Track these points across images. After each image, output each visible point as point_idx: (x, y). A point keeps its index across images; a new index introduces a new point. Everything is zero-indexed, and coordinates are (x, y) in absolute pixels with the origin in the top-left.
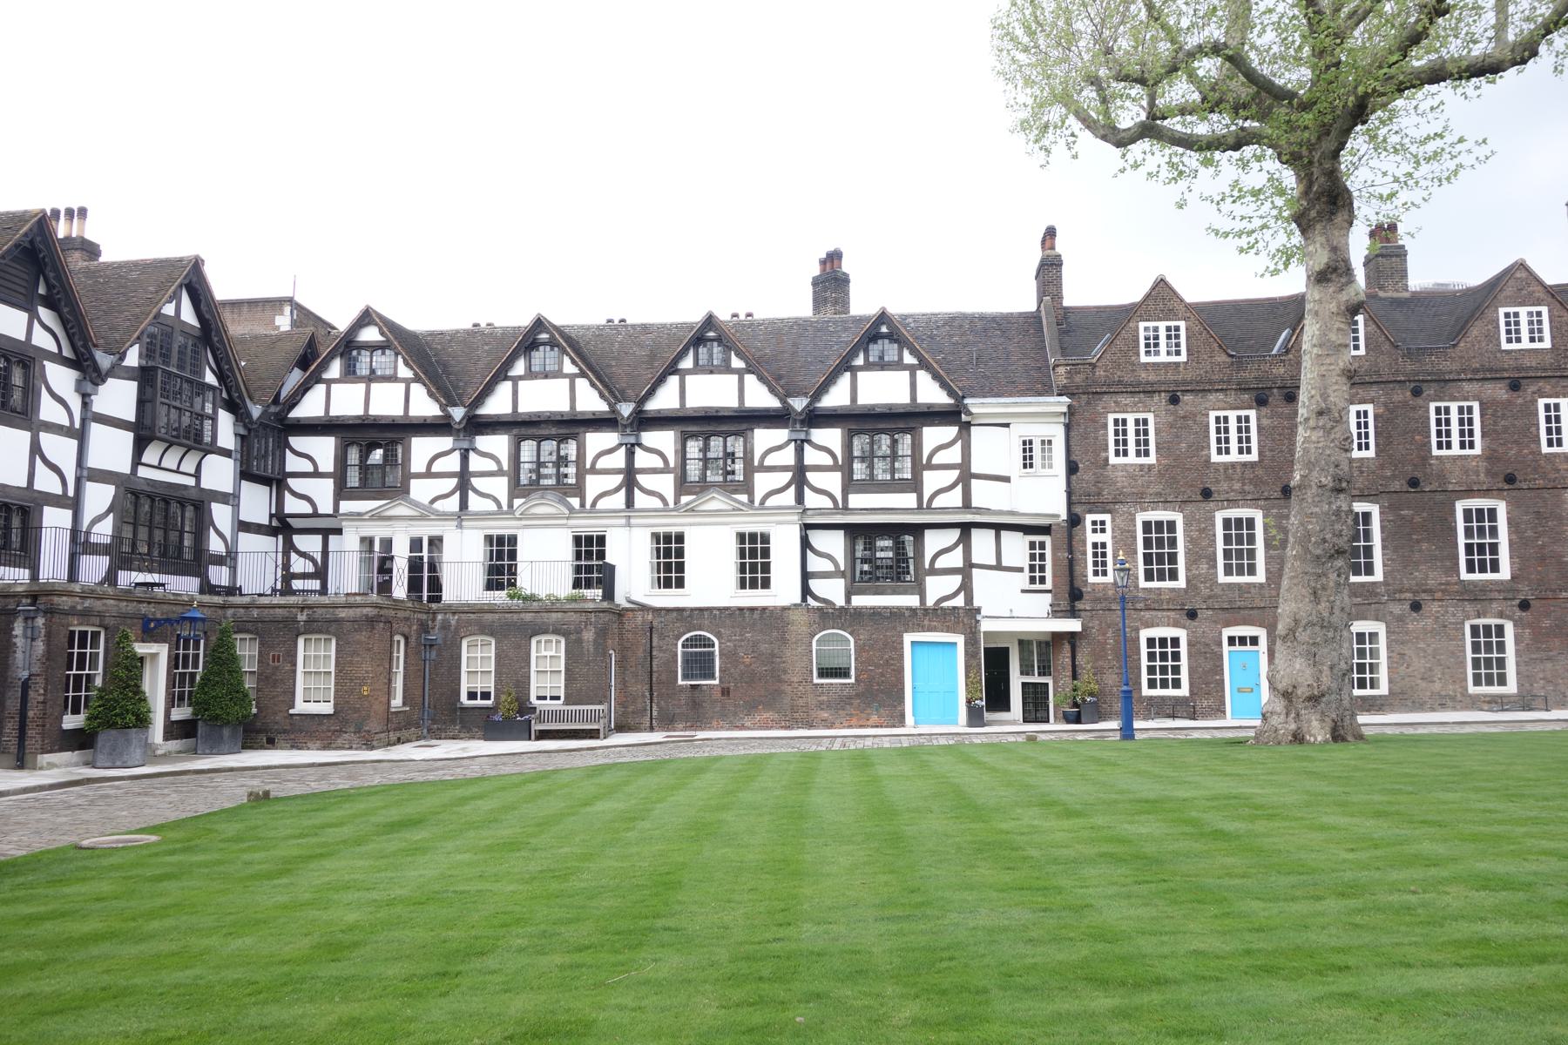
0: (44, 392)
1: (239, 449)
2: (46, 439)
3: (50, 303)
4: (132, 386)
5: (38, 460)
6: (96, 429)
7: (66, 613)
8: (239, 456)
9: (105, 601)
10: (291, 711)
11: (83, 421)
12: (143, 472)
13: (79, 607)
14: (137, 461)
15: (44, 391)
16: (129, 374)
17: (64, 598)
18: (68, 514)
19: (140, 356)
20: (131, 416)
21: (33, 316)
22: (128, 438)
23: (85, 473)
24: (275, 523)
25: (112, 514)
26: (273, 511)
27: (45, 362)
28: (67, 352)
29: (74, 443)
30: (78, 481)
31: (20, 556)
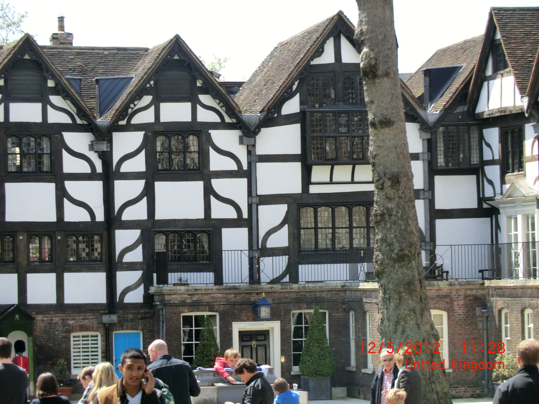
0: (212, 152)
1: (426, 150)
2: (217, 184)
3: (205, 91)
4: (295, 129)
5: (212, 198)
6: (261, 168)
7: (177, 305)
8: (426, 157)
9: (212, 295)
10: (363, 371)
11: (249, 164)
12: (313, 189)
13: (188, 301)
14: (306, 180)
15: (212, 152)
16: (290, 119)
17: (174, 296)
18: (244, 231)
19: (302, 103)
20: (297, 150)
21: (195, 102)
22: (297, 167)
23: (255, 200)
24: (485, 206)
25: (286, 226)
26: (481, 196)
27: (210, 131)
28: (228, 120)
29: (243, 182)
30: (250, 206)
31: (206, 264)
